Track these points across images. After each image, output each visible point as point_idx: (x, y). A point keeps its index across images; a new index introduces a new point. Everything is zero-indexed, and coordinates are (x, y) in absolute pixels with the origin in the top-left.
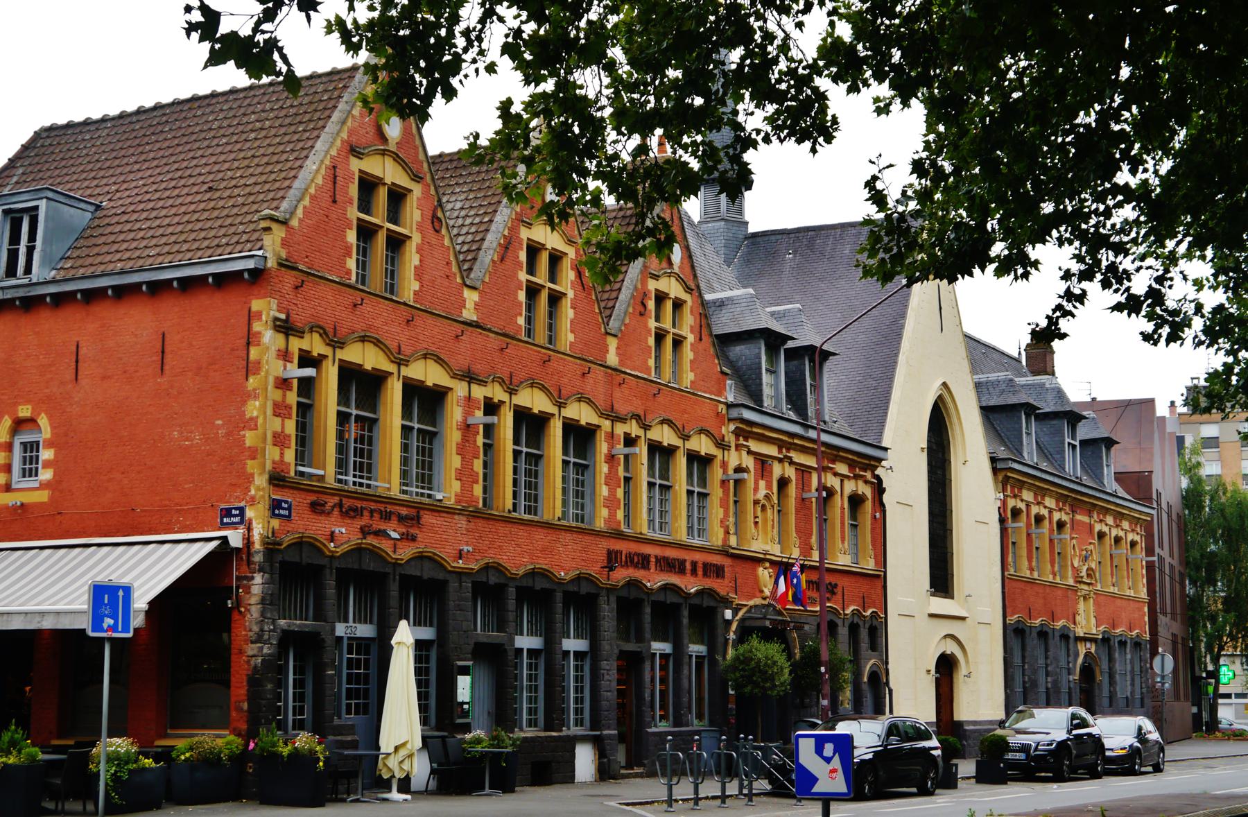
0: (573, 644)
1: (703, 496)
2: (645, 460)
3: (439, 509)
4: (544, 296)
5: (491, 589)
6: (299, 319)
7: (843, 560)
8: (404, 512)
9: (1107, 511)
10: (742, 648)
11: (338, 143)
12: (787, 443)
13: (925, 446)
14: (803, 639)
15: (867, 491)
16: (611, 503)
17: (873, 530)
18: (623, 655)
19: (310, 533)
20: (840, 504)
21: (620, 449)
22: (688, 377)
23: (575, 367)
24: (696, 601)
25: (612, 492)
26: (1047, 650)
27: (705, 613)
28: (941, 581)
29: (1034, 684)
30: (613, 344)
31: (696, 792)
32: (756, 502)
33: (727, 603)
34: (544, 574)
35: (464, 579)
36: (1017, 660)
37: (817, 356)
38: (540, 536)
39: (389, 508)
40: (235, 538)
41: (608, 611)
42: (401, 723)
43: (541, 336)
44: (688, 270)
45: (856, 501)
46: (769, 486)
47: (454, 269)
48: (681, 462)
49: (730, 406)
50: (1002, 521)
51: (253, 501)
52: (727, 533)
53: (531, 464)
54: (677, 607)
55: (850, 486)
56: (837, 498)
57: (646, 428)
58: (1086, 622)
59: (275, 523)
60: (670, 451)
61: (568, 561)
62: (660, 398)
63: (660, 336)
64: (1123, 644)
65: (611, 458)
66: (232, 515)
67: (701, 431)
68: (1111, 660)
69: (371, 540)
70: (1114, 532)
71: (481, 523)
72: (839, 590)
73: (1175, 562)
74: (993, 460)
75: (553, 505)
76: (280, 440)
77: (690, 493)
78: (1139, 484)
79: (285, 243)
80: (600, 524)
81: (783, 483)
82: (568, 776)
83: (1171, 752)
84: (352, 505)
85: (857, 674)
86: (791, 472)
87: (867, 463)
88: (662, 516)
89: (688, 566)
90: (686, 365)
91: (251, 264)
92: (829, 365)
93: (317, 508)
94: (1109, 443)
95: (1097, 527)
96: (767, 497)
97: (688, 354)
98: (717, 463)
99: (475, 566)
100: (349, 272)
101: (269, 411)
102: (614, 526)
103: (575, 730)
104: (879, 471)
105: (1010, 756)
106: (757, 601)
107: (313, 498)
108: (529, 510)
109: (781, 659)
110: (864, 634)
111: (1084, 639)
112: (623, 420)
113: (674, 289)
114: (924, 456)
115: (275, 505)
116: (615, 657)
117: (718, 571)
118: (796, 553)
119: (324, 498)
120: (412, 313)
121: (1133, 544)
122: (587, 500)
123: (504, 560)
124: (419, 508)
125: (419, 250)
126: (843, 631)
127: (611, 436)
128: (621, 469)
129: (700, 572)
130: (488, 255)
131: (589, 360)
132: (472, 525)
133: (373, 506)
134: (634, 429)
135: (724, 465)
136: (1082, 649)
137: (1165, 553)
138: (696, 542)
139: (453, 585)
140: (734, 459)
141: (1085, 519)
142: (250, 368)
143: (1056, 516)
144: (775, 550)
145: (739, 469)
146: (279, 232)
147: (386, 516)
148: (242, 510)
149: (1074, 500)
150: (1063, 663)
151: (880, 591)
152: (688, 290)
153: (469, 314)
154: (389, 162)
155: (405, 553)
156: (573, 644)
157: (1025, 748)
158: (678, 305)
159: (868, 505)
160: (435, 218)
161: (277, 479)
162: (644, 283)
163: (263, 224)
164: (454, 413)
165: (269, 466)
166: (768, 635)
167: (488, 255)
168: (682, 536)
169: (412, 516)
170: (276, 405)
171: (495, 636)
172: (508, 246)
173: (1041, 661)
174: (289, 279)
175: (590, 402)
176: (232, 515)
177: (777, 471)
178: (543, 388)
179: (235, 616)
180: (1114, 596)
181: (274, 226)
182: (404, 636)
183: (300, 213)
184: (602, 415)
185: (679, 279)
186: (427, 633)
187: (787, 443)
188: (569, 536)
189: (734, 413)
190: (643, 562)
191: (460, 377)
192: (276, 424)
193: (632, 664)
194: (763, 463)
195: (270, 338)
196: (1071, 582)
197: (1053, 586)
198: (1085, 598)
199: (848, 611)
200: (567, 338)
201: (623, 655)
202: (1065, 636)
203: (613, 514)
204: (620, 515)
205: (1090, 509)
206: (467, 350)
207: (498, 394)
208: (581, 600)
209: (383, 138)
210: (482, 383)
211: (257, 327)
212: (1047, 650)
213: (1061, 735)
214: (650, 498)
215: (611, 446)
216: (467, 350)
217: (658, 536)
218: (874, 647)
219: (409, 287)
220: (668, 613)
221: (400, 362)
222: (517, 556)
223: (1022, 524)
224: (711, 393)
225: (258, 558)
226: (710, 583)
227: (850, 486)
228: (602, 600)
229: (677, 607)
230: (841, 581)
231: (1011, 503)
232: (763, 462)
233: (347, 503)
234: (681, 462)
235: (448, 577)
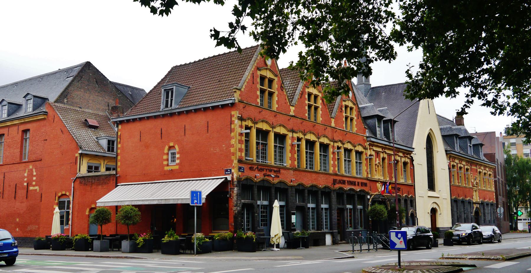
0: (324, 206)
1: (360, 163)
2: (343, 153)
3: (285, 168)
4: (313, 108)
5: (300, 190)
6: (245, 117)
7: (402, 181)
8: (275, 169)
9: (481, 165)
10: (373, 207)
11: (254, 67)
12: (384, 147)
13: (425, 147)
14: (391, 204)
16: (334, 165)
17: (410, 172)
18: (339, 209)
19: (250, 176)
20: (400, 165)
21: (336, 150)
22: (355, 129)
23: (323, 127)
24: (359, 193)
25: (334, 163)
26: (464, 207)
27: (362, 197)
28: (431, 186)
29: (461, 216)
30: (333, 120)
31: (361, 248)
32: (376, 165)
33: (368, 194)
34: (315, 186)
36: (455, 209)
37: (393, 122)
38: (314, 175)
39: (271, 168)
40: (229, 178)
41: (334, 197)
42: (276, 228)
43: (313, 119)
44: (354, 99)
45: (405, 164)
46: (379, 160)
47: (287, 101)
48: (354, 154)
49: (367, 137)
50: (449, 169)
51: (234, 167)
52: (368, 173)
53: (311, 155)
54: (354, 195)
55: (403, 160)
56: (400, 163)
57: (343, 144)
58: (476, 198)
59: (240, 173)
60: (350, 151)
61: (322, 182)
62: (347, 135)
63: (346, 118)
64: (487, 204)
65: (333, 153)
66: (228, 171)
67: (359, 145)
68: (484, 209)
69: (266, 178)
70: (484, 171)
71: (297, 172)
72: (401, 190)
73: (503, 180)
74: (446, 151)
75: (317, 166)
76: (240, 150)
77: (356, 162)
78: (491, 157)
79: (240, 95)
80: (331, 172)
81: (384, 159)
82: (324, 244)
83: (504, 236)
84: (261, 168)
85: (407, 214)
86: (386, 156)
87: (408, 153)
88: (349, 169)
89: (357, 183)
90: (354, 126)
91: (231, 102)
92: (396, 124)
93: (251, 169)
94: (482, 145)
95: (479, 170)
96: (379, 163)
97: (355, 123)
98: (364, 154)
99: (296, 184)
100: (258, 103)
101: (237, 142)
103: (325, 230)
104: (412, 155)
105: (454, 238)
106: (377, 193)
107: (250, 166)
108: (310, 168)
109: (384, 210)
110: (409, 202)
111: (476, 203)
112: (337, 142)
113: (350, 104)
114: (425, 150)
115: (240, 168)
117: (365, 185)
118: (388, 179)
119: (253, 166)
120: (276, 114)
121: (490, 175)
122: (327, 165)
123: (304, 182)
124: (279, 168)
125: (277, 96)
126: (403, 201)
127: (333, 147)
128: (336, 156)
129: (360, 185)
130: (297, 96)
131: (326, 125)
133: (267, 168)
134: (340, 144)
135: (366, 154)
136: (475, 206)
137: (500, 177)
138: (359, 176)
139: (290, 190)
140: (369, 152)
141: (475, 168)
142: (232, 130)
143: (466, 167)
144: (382, 178)
145: (370, 155)
146: (238, 92)
147: (271, 171)
148: (231, 170)
149: (471, 162)
150: (469, 210)
151: (413, 189)
152: (354, 104)
153: (292, 113)
154: (268, 71)
155: (276, 181)
156: (324, 206)
157: (458, 235)
158: (351, 109)
159: (409, 165)
160: (281, 87)
161: (240, 161)
162: (341, 103)
163: (234, 90)
164: (289, 141)
165: (238, 158)
166: (380, 203)
167: (297, 96)
168: (355, 175)
169: (278, 170)
170: (239, 141)
171: (302, 204)
172: (302, 94)
173: (462, 210)
174: (242, 105)
175: (327, 137)
176: (228, 171)
177: (382, 155)
178: (313, 134)
179: (230, 199)
180: (484, 190)
181: (237, 91)
182: (277, 204)
183: (244, 87)
184: (331, 141)
185: (351, 101)
186: (283, 203)
187: (384, 147)
189: (369, 139)
190: (344, 182)
191: (290, 131)
192: (239, 146)
193: (341, 211)
194: (378, 153)
195: (237, 122)
196: (471, 186)
197: (465, 187)
198: (475, 191)
199: (404, 196)
200: (320, 119)
201: (339, 209)
202: (470, 202)
203: (334, 169)
204: (337, 169)
205: (476, 165)
206: (292, 123)
207: (301, 136)
208: (326, 193)
209: (266, 65)
210: (296, 133)
211: (233, 119)
212: (464, 207)
213: (469, 231)
214: (345, 164)
215: (333, 150)
216: (292, 123)
217: (347, 175)
218: (412, 206)
219: (275, 106)
220: (351, 197)
221: (273, 128)
222: (308, 181)
223: (455, 169)
225: (236, 183)
226: (363, 188)
227: (403, 160)
228: (332, 193)
229: (354, 195)
230: (402, 187)
231: (452, 163)
232: (377, 153)
233: (260, 167)
234: (354, 154)
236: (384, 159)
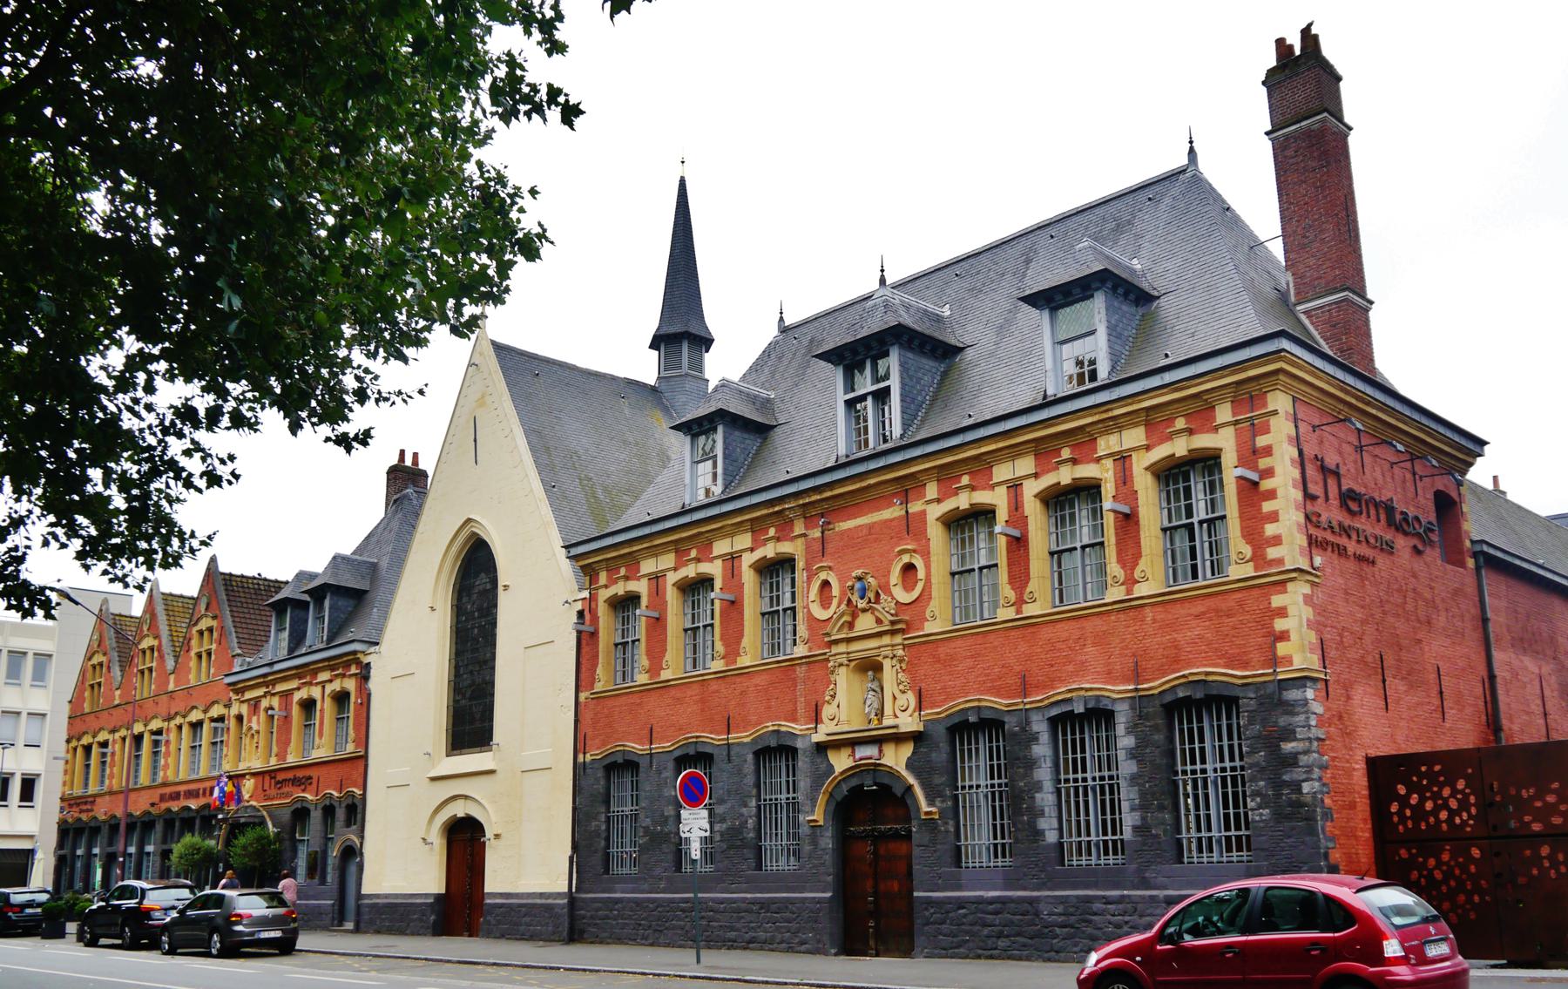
15: (350, 685)
20: (326, 708)
45: (341, 698)
61: (140, 805)
72: (314, 781)
110: (340, 814)
229: (193, 819)
230: (313, 773)
232: (255, 704)
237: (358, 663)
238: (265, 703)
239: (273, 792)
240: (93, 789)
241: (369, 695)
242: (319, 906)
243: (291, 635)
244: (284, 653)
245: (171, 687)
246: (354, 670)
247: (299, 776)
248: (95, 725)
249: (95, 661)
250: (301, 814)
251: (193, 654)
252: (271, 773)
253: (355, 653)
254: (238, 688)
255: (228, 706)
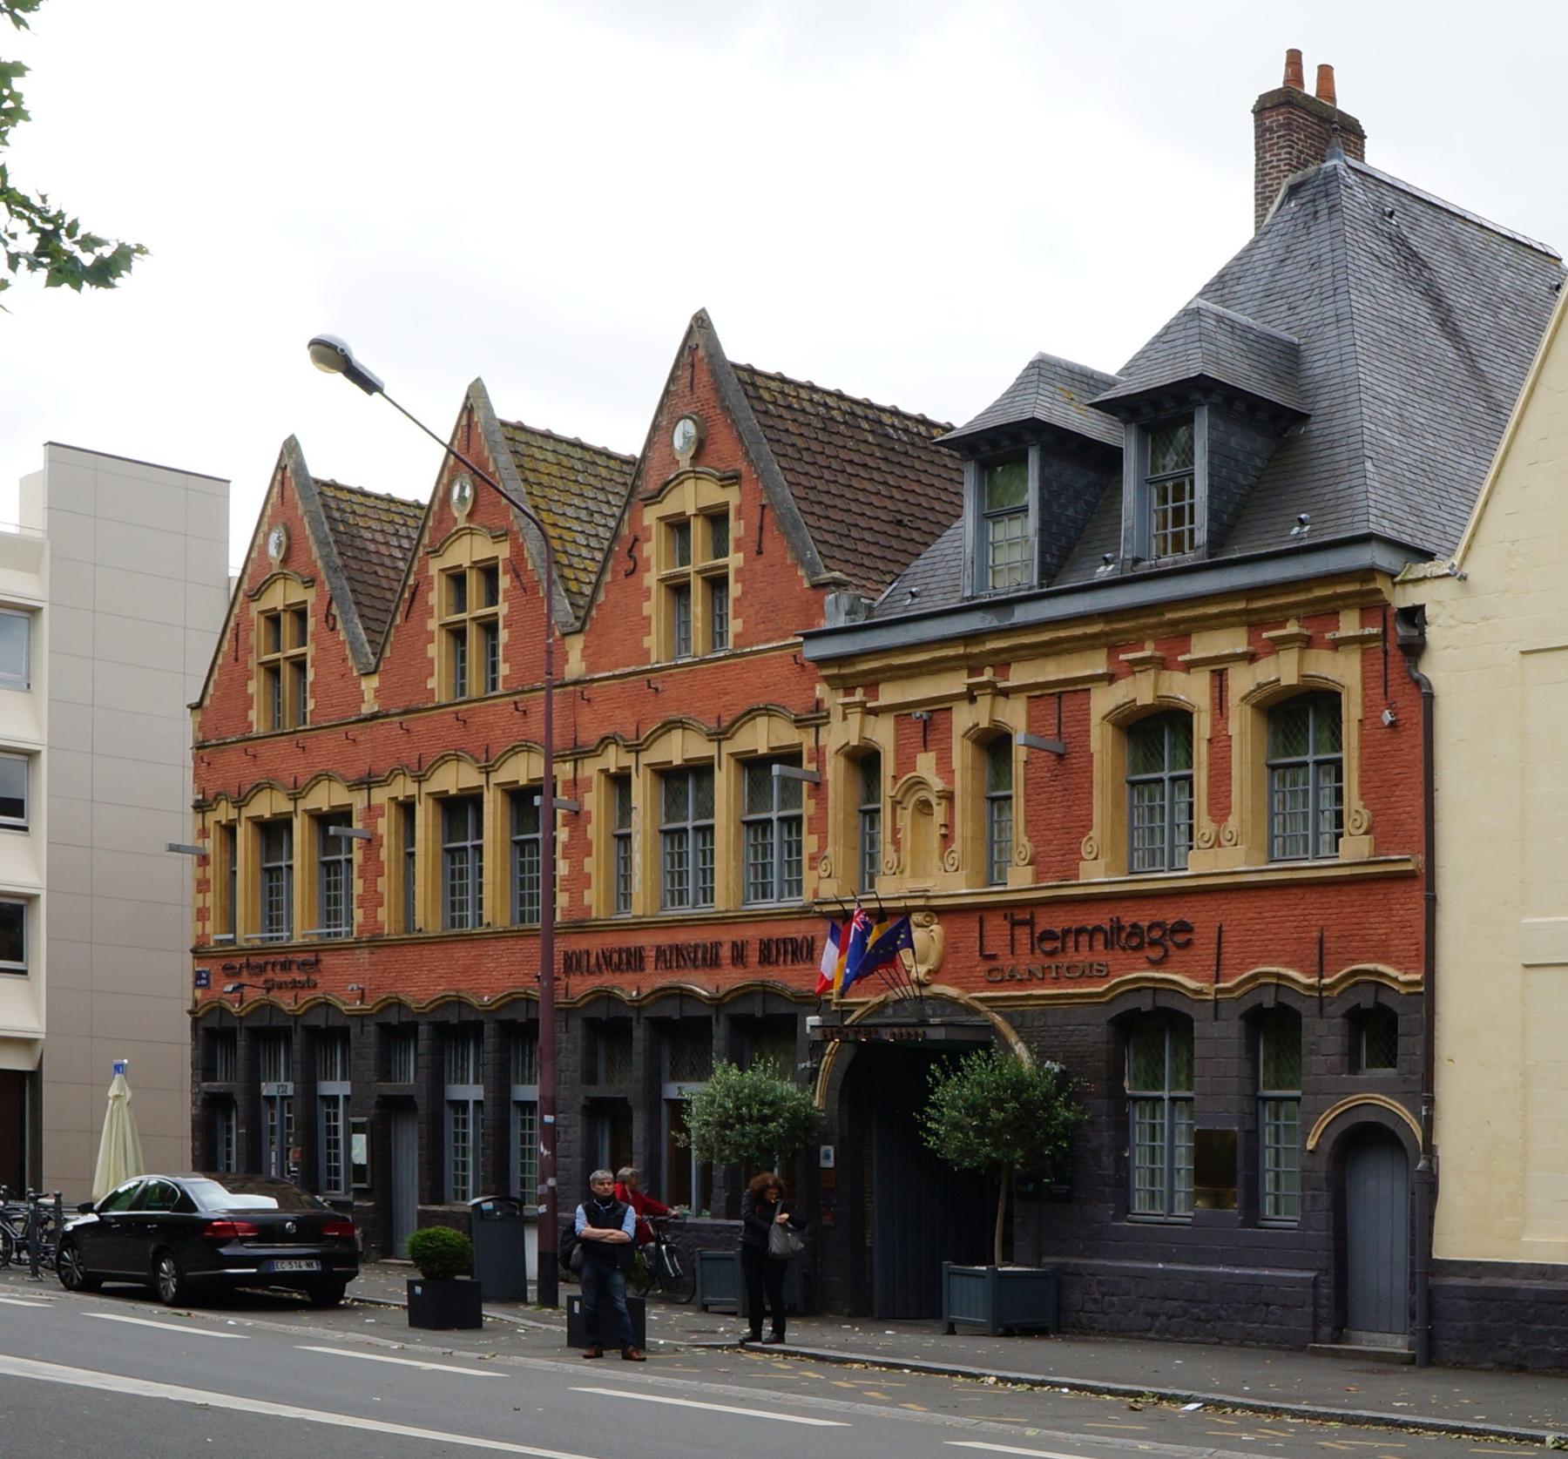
5: (395, 1030)
35: (366, 1021)
53: (459, 861)
59: (198, 993)
75: (495, 905)
89: (726, 952)
102: (577, 916)
116: (577, 1107)
132: (375, 958)
188: (502, 945)
190: (633, 960)
208: (515, 1031)
220: (683, 1034)
222: (422, 985)
224: (766, 641)
229: (706, 1022)
230: (1201, 917)
235: (349, 1023)
236: (994, 744)
237: (1371, 606)
238: (965, 718)
239: (1026, 960)
240: (302, 927)
241: (1429, 699)
242: (1255, 1283)
243: (1044, 529)
244: (1030, 578)
245: (575, 666)
246: (1349, 625)
247: (1154, 921)
248: (295, 767)
249: (276, 598)
250: (1153, 1026)
251: (651, 579)
252: (1018, 913)
253: (1369, 573)
254: (851, 675)
255: (814, 718)
